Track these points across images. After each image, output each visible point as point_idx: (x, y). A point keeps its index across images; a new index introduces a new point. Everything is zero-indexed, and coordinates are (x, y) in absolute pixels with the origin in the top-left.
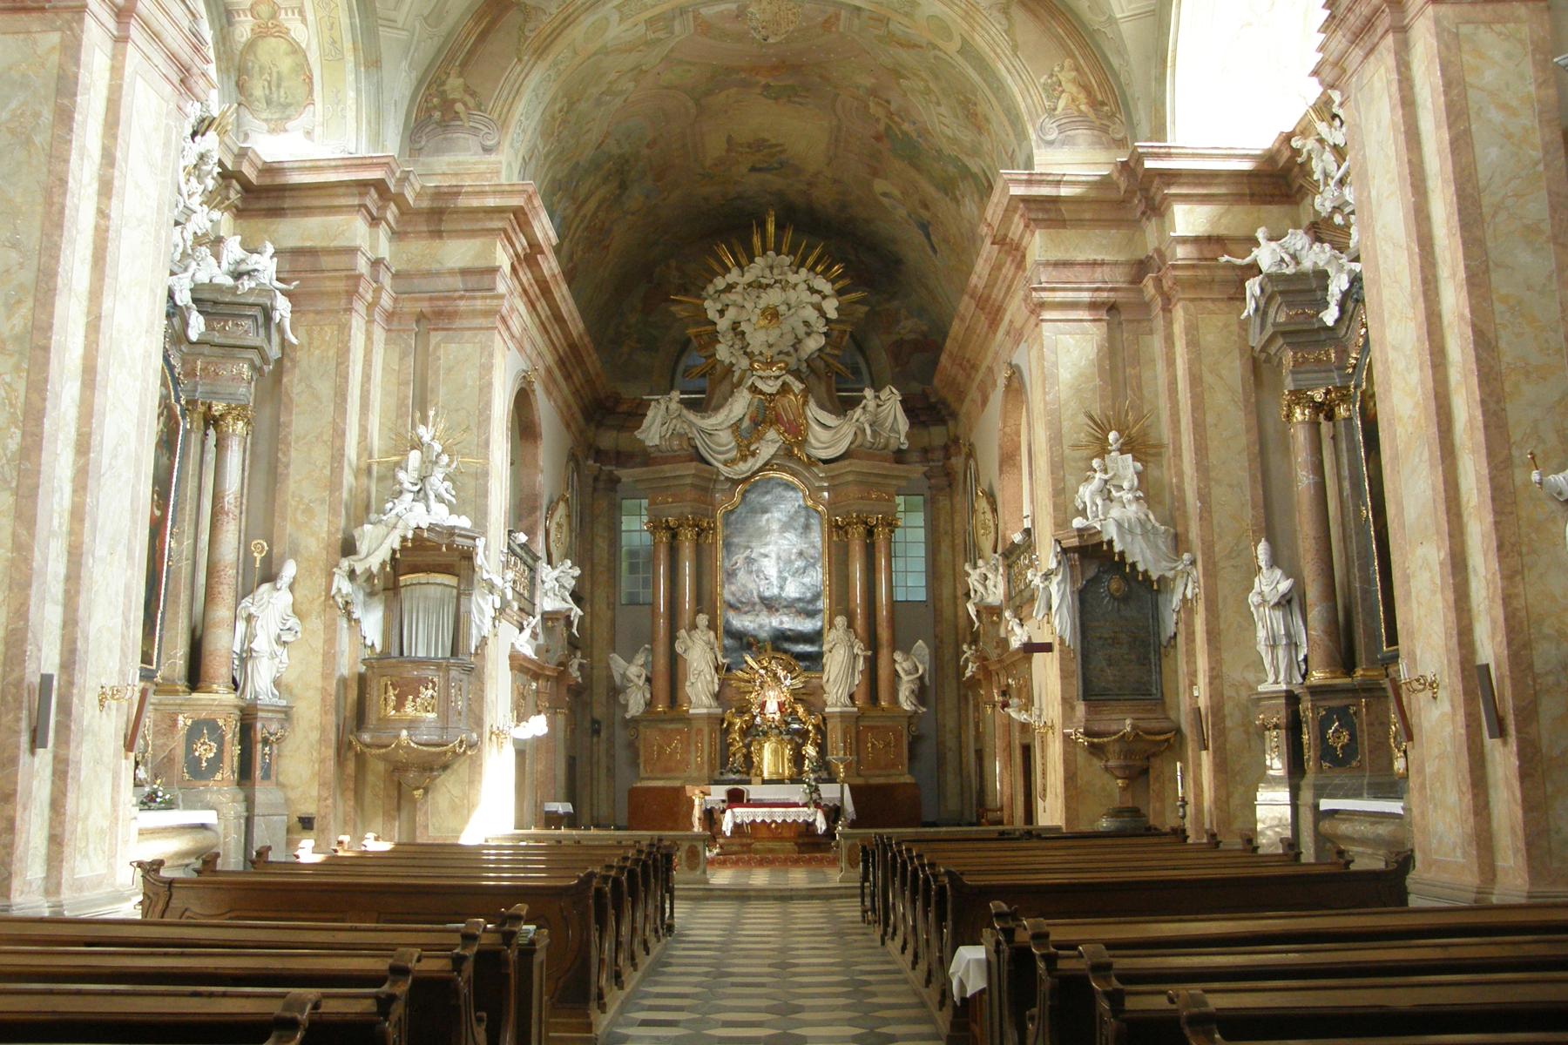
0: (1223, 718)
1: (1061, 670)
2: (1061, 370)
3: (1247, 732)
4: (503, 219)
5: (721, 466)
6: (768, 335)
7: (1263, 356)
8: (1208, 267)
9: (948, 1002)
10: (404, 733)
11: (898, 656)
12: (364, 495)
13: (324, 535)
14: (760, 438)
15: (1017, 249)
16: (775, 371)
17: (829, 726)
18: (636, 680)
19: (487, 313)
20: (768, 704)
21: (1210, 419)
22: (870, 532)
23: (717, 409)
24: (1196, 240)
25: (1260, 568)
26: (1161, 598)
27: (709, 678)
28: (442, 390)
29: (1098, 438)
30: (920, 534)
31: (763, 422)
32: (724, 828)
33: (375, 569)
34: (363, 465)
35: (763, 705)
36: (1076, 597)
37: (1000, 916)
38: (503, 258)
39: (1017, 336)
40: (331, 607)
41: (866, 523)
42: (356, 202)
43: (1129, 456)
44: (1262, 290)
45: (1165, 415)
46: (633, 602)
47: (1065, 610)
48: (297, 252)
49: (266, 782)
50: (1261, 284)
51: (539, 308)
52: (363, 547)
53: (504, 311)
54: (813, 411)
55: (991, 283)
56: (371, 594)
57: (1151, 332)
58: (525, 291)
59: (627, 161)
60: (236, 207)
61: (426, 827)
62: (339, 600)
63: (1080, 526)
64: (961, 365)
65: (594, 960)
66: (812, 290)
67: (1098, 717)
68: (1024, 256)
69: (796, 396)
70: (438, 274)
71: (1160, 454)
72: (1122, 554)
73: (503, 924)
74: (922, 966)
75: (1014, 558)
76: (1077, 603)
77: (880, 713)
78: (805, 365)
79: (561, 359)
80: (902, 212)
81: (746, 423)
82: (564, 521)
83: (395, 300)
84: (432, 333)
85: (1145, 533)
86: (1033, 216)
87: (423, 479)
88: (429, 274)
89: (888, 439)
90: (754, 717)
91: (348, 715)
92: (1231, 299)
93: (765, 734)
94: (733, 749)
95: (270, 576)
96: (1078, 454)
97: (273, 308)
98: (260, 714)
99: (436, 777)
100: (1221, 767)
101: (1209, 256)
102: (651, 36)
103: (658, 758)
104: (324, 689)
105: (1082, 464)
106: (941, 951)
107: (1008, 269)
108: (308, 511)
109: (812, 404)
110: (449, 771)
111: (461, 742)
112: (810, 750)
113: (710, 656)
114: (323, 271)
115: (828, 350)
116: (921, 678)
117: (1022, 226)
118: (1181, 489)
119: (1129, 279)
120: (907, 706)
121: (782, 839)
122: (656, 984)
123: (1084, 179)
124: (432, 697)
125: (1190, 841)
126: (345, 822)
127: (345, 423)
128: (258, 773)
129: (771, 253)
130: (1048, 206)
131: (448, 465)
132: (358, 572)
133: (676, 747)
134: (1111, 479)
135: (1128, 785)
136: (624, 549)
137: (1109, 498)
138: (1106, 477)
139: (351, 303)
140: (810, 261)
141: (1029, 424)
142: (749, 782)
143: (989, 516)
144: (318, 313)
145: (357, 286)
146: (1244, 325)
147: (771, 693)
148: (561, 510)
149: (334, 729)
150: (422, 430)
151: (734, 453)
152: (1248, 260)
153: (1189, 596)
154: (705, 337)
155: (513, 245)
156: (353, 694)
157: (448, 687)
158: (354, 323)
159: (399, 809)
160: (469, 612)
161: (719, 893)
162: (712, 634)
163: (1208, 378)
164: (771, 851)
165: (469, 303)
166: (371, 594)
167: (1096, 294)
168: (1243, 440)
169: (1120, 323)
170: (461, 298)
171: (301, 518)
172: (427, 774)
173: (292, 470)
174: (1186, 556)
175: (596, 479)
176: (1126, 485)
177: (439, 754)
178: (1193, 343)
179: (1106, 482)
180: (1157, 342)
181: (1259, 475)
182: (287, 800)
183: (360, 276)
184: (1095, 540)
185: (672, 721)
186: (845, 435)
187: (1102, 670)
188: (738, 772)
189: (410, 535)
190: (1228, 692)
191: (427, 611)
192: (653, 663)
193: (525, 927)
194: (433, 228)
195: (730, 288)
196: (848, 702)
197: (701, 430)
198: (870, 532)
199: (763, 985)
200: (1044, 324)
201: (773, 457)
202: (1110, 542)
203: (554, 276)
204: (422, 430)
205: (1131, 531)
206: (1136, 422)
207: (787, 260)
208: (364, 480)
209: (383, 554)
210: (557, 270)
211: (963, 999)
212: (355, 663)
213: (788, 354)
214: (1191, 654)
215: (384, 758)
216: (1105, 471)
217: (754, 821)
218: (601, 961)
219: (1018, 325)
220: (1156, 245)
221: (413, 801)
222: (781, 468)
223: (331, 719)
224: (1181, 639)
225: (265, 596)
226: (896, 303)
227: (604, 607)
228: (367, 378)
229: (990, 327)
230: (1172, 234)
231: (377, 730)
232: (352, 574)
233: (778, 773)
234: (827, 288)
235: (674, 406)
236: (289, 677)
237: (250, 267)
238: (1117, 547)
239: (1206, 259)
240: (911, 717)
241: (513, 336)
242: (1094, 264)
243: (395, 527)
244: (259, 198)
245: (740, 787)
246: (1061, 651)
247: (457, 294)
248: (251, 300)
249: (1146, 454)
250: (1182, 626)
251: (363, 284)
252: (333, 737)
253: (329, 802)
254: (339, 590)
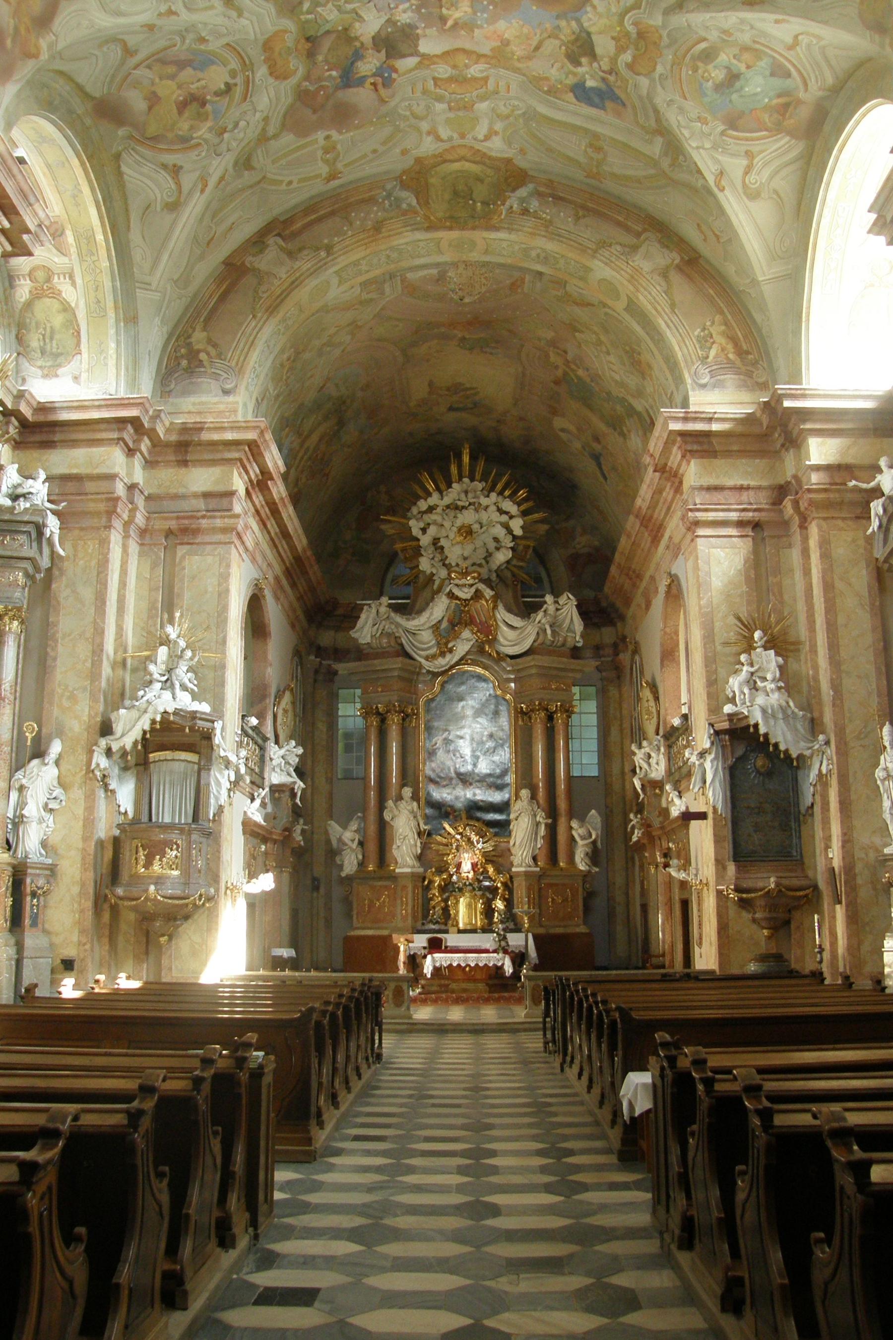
0: (854, 877)
1: (715, 835)
2: (713, 579)
3: (875, 889)
4: (239, 451)
5: (423, 661)
6: (463, 549)
7: (886, 566)
8: (838, 491)
9: (619, 1120)
10: (152, 888)
11: (574, 824)
12: (120, 685)
13: (86, 718)
14: (457, 636)
15: (675, 475)
16: (469, 580)
17: (515, 885)
18: (350, 843)
19: (225, 530)
20: (463, 865)
21: (841, 620)
22: (550, 718)
23: (420, 612)
24: (828, 468)
25: (885, 747)
26: (800, 773)
27: (412, 842)
28: (187, 595)
29: (745, 637)
30: (593, 720)
31: (459, 623)
32: (425, 971)
33: (128, 747)
34: (119, 658)
35: (459, 866)
36: (727, 772)
37: (665, 1045)
38: (239, 484)
39: (676, 550)
40: (91, 779)
41: (547, 710)
42: (115, 435)
43: (772, 652)
44: (885, 510)
45: (802, 618)
46: (348, 776)
47: (717, 784)
48: (65, 478)
49: (34, 929)
50: (883, 505)
51: (269, 526)
52: (118, 728)
53: (240, 528)
54: (502, 614)
55: (653, 505)
56: (125, 769)
57: (790, 546)
58: (257, 512)
59: (344, 402)
60: (15, 440)
61: (170, 969)
62: (98, 773)
63: (730, 711)
64: (627, 575)
65: (314, 1085)
66: (501, 511)
67: (747, 876)
68: (681, 483)
69: (487, 601)
70: (184, 497)
71: (798, 650)
72: (766, 735)
73: (236, 1050)
74: (596, 1090)
75: (673, 739)
76: (728, 778)
77: (558, 873)
78: (494, 575)
79: (287, 569)
80: (577, 445)
81: (445, 624)
82: (289, 707)
83: (148, 519)
84: (179, 547)
85: (786, 717)
86: (689, 448)
87: (170, 671)
88: (176, 497)
89: (565, 640)
90: (451, 876)
91: (104, 871)
92: (858, 518)
93: (460, 890)
94: (433, 903)
95: (39, 753)
96: (728, 650)
97: (44, 525)
98: (29, 871)
99: (178, 926)
100: (852, 919)
101: (838, 481)
102: (365, 296)
103: (369, 911)
104: (84, 849)
105: (731, 659)
106: (613, 1076)
107: (668, 493)
108: (73, 698)
109: (501, 607)
110: (190, 921)
111: (201, 895)
112: (499, 904)
113: (413, 823)
114: (86, 494)
115: (515, 562)
116: (594, 843)
117: (679, 456)
118: (816, 679)
119: (770, 501)
120: (582, 866)
121: (475, 981)
122: (368, 1104)
123: (732, 416)
124: (176, 857)
125: (826, 982)
126: (101, 965)
127: (104, 623)
128: (27, 922)
129: (466, 480)
130: (701, 439)
131: (191, 659)
132: (114, 750)
134: (757, 671)
135: (772, 935)
136: (340, 732)
137: (754, 688)
138: (752, 670)
139: (110, 521)
140: (499, 487)
141: (686, 624)
142: (446, 932)
143: (652, 703)
144: (82, 529)
145: (115, 507)
146: (869, 540)
147: (466, 855)
148: (287, 698)
149: (92, 884)
150: (169, 629)
151: (434, 650)
152: (872, 484)
153: (824, 771)
154: (410, 552)
155: (247, 472)
156: (109, 854)
157: (189, 848)
158: (113, 538)
159: (147, 953)
160: (208, 784)
161: (422, 1027)
162: (415, 804)
163: (839, 585)
164: (465, 990)
165: (210, 521)
166: (125, 769)
167: (743, 514)
168: (869, 639)
169: (763, 539)
170: (203, 517)
171: (66, 703)
172: (171, 923)
173: (59, 662)
174: (821, 737)
175: (316, 672)
176: (769, 676)
177: (182, 905)
178: (826, 556)
179: (752, 674)
180: (795, 554)
181: (883, 669)
182: (52, 945)
183: (118, 499)
184: (743, 724)
185: (381, 878)
186: (529, 635)
187: (749, 835)
188: (437, 922)
189: (158, 718)
190: (859, 854)
191: (172, 784)
192: (365, 830)
193: (255, 1053)
194: (180, 458)
195: (431, 509)
196: (531, 862)
197: (407, 631)
198: (550, 718)
199: (458, 1106)
200: (698, 539)
201: (467, 653)
202: (756, 726)
203: (282, 499)
204: (169, 629)
205: (774, 716)
206: (777, 623)
207: (479, 486)
208: (120, 672)
209: (135, 734)
210: (284, 493)
211: (633, 1119)
212: (111, 828)
213: (480, 565)
214: (826, 822)
215: (134, 909)
216: (752, 665)
217: (451, 965)
218: (320, 1084)
219: (676, 540)
220: (794, 472)
221: (160, 947)
222: (474, 663)
223: (90, 875)
224: (817, 809)
225: (35, 770)
226: (572, 523)
228: (123, 584)
229: (653, 542)
230: (807, 463)
231: (129, 885)
232: (109, 752)
233: (471, 924)
234: (513, 509)
235: (383, 609)
236: (54, 840)
237: (25, 491)
238: (762, 730)
239: (837, 484)
240: (586, 875)
241: (246, 549)
242: (741, 488)
243: (145, 711)
244: (33, 433)
245: (439, 936)
246: (714, 819)
247: (200, 514)
248: (26, 518)
249: (786, 650)
250: (818, 798)
251: (120, 504)
252: (91, 891)
253: (88, 947)
254: (98, 765)
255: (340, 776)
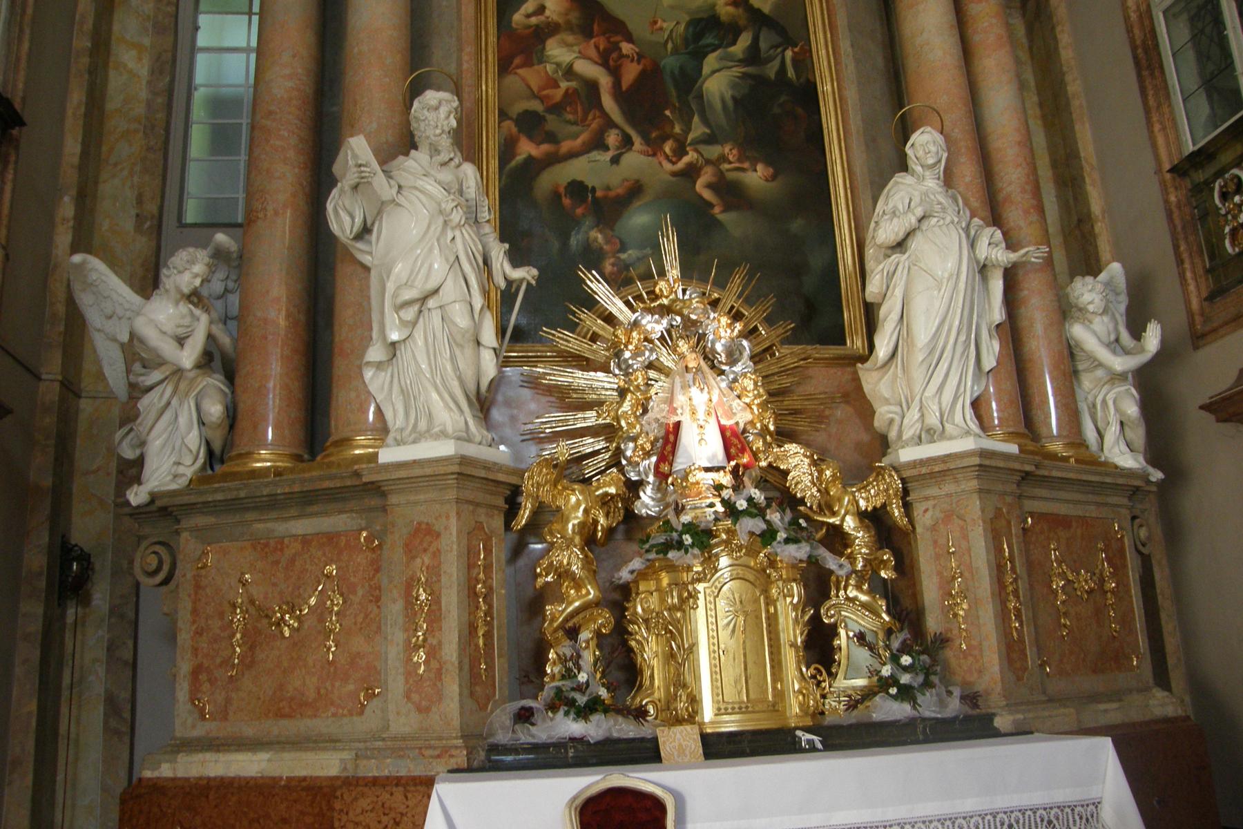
17: (924, 517)
18: (167, 348)
20: (688, 437)
27: (462, 321)
90: (634, 488)
93: (703, 536)
94: (557, 612)
103: (248, 662)
133: (321, 612)
136: (199, 95)
147: (699, 397)
185: (308, 500)
227: (129, 225)
255: (190, 218)
